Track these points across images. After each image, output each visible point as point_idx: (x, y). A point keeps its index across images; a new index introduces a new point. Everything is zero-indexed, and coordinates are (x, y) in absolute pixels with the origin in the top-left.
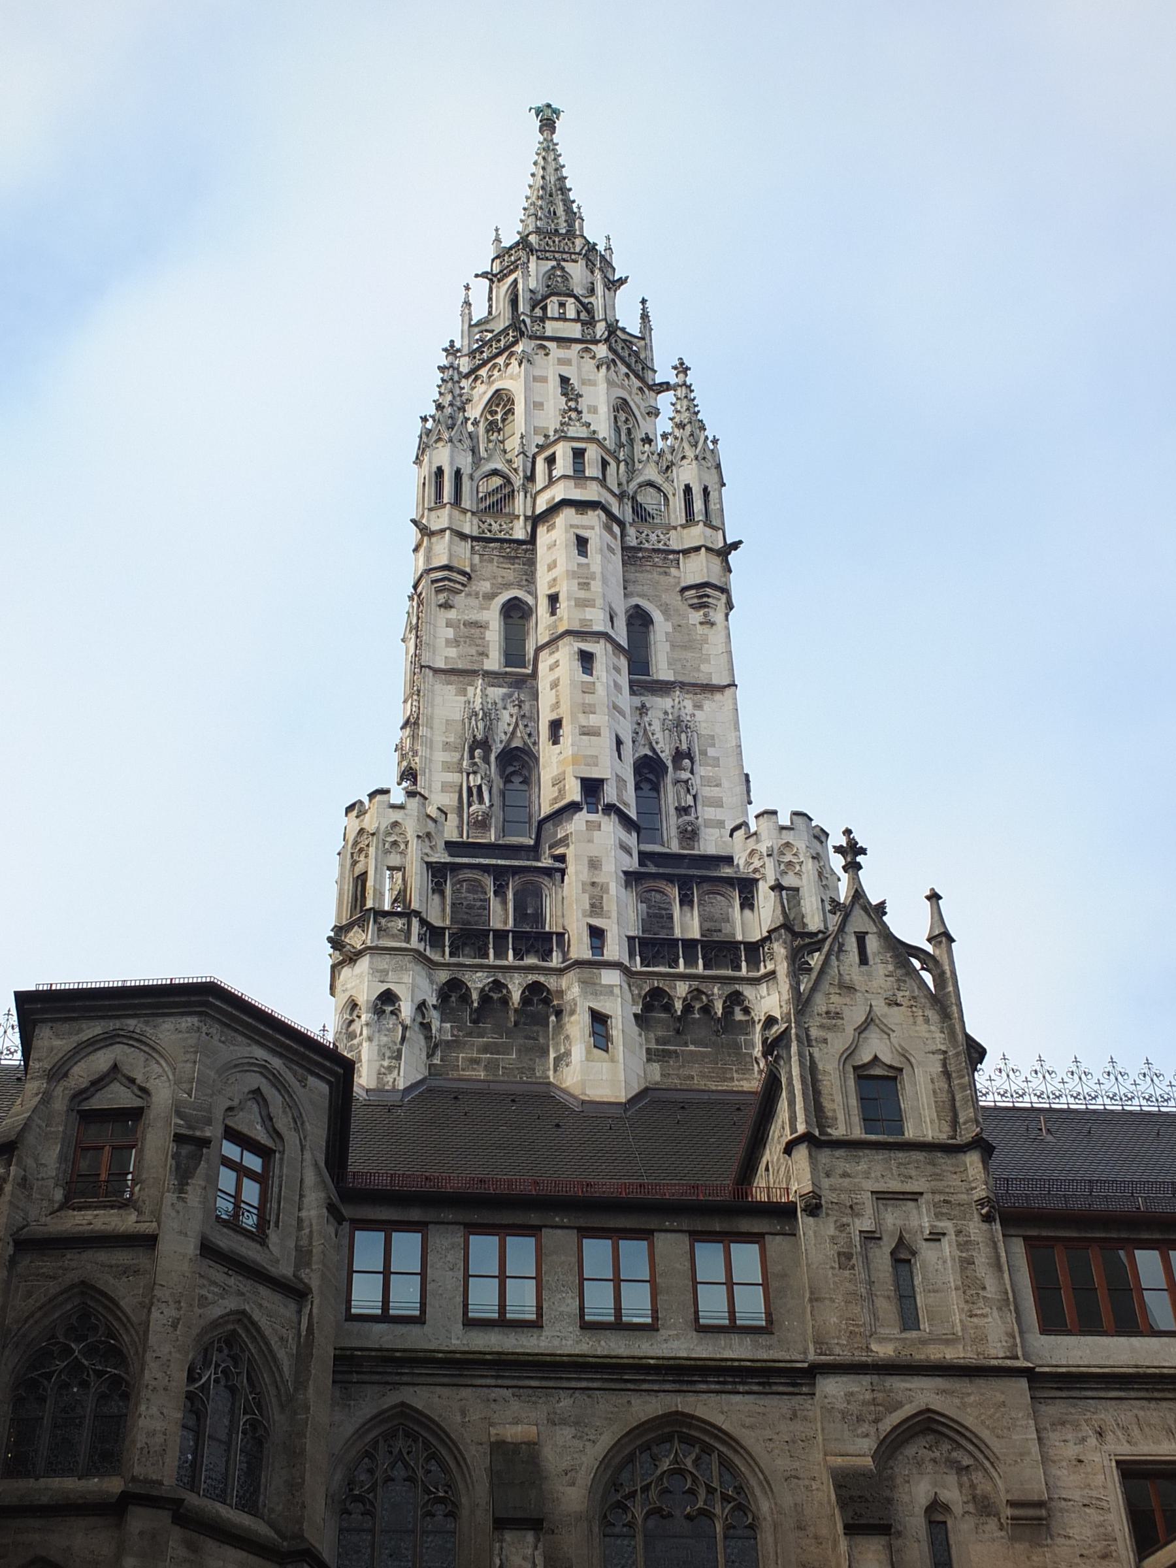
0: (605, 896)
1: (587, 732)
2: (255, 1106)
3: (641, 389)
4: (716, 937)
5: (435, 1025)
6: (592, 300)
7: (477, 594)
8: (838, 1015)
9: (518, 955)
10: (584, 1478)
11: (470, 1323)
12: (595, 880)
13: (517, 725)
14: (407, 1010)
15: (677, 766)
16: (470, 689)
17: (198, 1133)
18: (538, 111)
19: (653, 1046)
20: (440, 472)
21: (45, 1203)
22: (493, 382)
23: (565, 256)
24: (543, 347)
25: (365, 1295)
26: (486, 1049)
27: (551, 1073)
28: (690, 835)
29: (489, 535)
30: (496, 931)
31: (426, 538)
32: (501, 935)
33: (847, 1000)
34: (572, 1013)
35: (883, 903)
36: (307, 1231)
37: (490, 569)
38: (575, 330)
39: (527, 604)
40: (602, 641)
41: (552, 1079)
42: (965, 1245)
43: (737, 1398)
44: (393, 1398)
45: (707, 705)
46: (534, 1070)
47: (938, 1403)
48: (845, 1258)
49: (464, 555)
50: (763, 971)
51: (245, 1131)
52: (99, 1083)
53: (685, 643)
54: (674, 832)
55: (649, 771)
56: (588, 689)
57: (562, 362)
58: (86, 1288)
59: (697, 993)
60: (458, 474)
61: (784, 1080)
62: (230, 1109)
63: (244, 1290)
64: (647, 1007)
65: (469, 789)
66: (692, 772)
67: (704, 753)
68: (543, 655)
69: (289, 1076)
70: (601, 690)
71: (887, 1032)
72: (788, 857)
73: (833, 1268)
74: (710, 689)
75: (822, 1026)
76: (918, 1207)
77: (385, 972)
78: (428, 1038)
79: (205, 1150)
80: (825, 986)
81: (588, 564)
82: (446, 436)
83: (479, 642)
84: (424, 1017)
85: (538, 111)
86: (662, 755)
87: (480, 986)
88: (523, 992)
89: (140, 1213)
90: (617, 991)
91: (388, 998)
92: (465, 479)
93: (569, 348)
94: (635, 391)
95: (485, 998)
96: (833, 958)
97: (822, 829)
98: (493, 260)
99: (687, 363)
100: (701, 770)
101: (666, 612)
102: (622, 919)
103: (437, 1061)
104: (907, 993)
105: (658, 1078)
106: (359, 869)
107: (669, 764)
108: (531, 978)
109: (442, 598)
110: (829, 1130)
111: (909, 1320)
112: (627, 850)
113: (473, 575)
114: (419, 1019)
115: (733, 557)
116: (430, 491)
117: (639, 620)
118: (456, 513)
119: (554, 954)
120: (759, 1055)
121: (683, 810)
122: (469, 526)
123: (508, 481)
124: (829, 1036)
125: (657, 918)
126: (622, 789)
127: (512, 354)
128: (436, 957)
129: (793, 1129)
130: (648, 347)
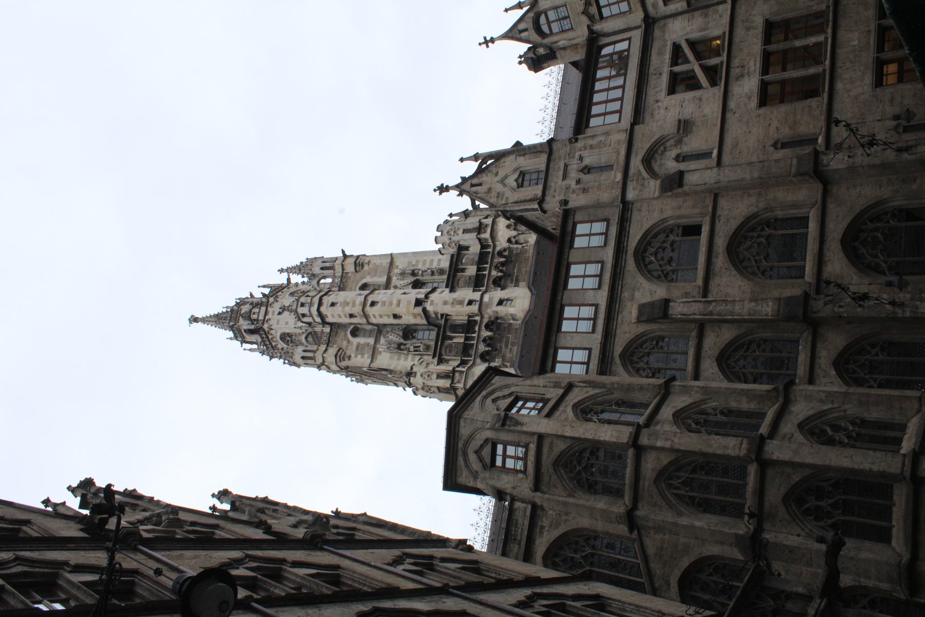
4: (477, 259)
8: (498, 194)
10: (653, 287)
11: (593, 331)
18: (191, 323)
20: (303, 358)
25: (578, 370)
26: (506, 346)
28: (441, 272)
32: (467, 339)
38: (263, 309)
42: (585, 148)
43: (631, 231)
44: (617, 360)
47: (640, 157)
48: (585, 190)
49: (332, 351)
52: (481, 460)
53: (375, 272)
55: (417, 285)
56: (384, 303)
58: (556, 464)
60: (304, 351)
64: (499, 286)
69: (490, 389)
71: (506, 177)
74: (392, 263)
80: (487, 198)
85: (191, 323)
95: (488, 345)
100: (420, 267)
101: (363, 278)
102: (466, 293)
103: (508, 364)
106: (436, 390)
108: (483, 328)
111: (609, 167)
115: (347, 253)
117: (364, 287)
121: (433, 273)
122: (323, 347)
123: (310, 333)
126: (420, 293)
128: (471, 363)
129: (536, 210)
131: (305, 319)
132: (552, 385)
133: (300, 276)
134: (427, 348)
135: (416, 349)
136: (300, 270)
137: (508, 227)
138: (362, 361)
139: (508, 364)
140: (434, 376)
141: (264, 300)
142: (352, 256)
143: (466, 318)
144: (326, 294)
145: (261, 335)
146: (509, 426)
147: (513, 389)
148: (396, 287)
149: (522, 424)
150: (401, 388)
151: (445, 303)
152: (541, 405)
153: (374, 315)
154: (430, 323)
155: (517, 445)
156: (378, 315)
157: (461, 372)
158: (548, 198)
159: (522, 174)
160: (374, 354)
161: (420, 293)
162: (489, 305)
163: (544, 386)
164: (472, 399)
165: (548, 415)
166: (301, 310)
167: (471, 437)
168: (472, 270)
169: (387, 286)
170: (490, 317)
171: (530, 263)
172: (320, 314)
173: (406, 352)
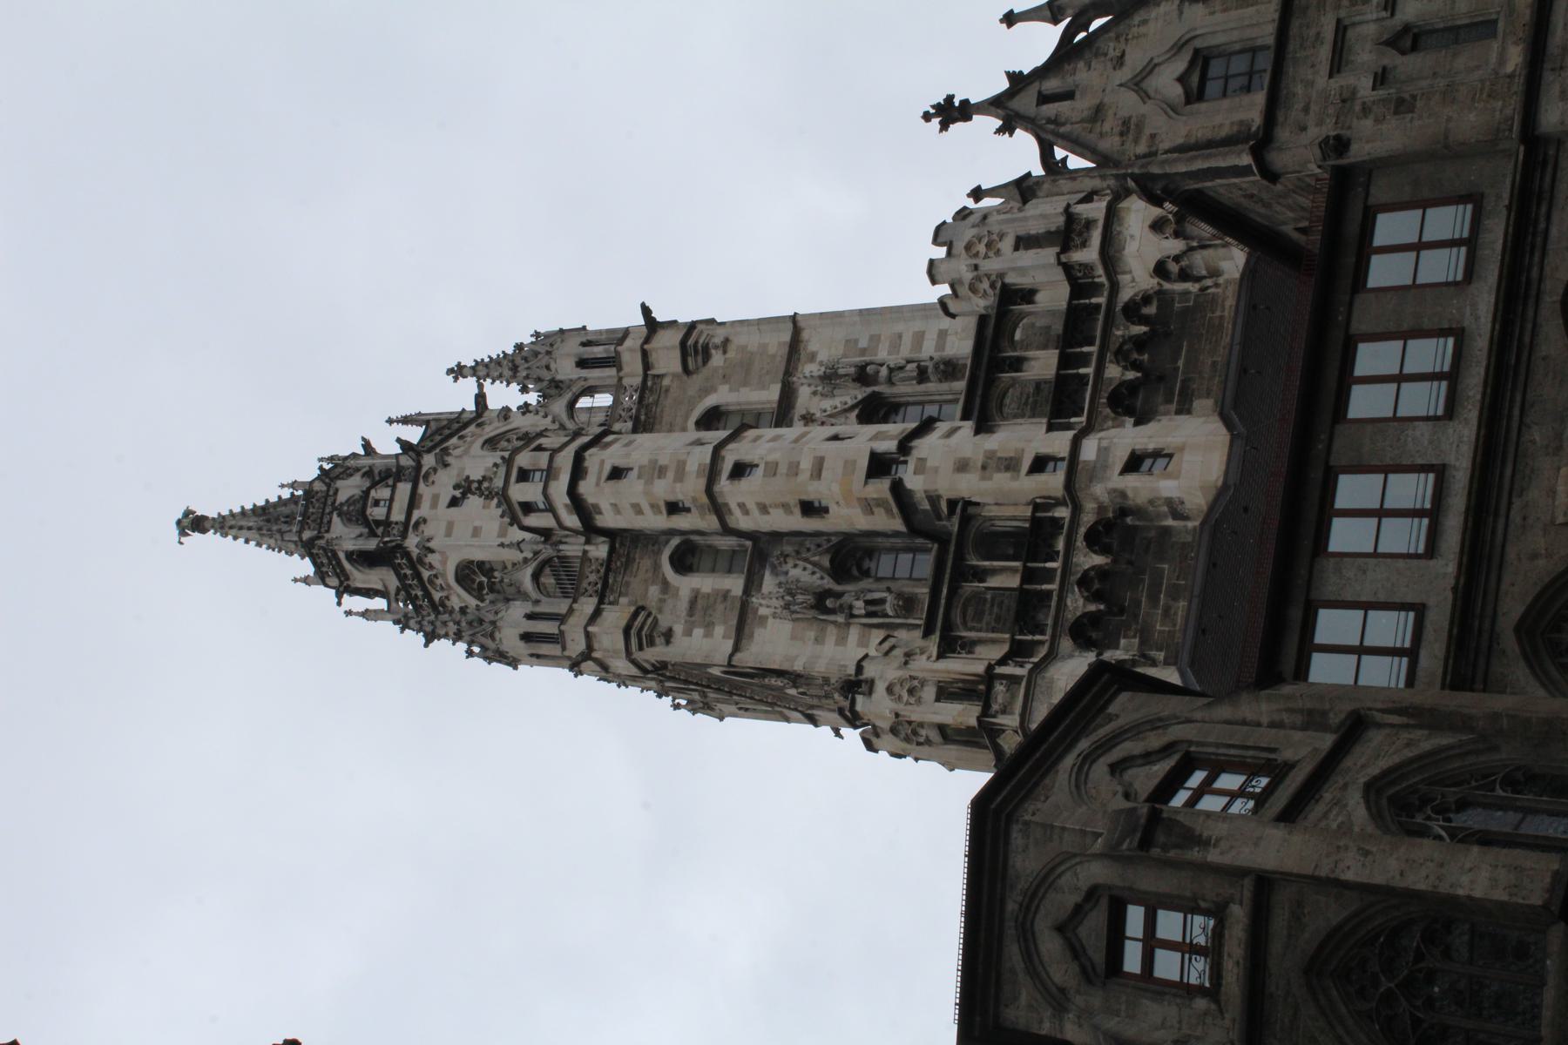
1: (818, 470)
2: (1130, 772)
4: (1058, 327)
7: (662, 601)
8: (1126, 123)
11: (1431, 550)
13: (806, 560)
16: (762, 611)
17: (1143, 821)
19: (1173, 407)
20: (527, 637)
21: (1209, 1020)
22: (449, 586)
25: (1382, 674)
26: (1154, 599)
27: (1190, 524)
28: (948, 369)
30: (1024, 580)
31: (595, 655)
32: (1029, 576)
33: (1111, 113)
34: (1123, 494)
36: (1285, 717)
37: (636, 583)
38: (404, 489)
39: (678, 547)
40: (723, 453)
41: (1197, 523)
43: (1554, 232)
44: (1509, 642)
45: (812, 347)
46: (1184, 544)
48: (1402, 106)
49: (615, 617)
50: (1103, 280)
51: (1156, 781)
52: (1076, 951)
54: (945, 386)
55: (874, 410)
56: (772, 469)
57: (434, 505)
59: (1121, 356)
60: (530, 617)
62: (1127, 796)
63: (1341, 782)
64: (1130, 412)
65: (869, 615)
67: (863, 351)
69: (1102, 732)
70: (771, 458)
71: (1151, 68)
72: (982, 248)
73: (1412, 120)
74: (795, 345)
75: (1136, 141)
76: (1354, 24)
79: (1165, 815)
80: (1091, 138)
81: (641, 467)
85: (183, 533)
87: (1081, 602)
88: (1095, 552)
89: (1231, 900)
90: (1105, 443)
92: (538, 609)
94: (478, 431)
95: (1096, 597)
96: (1062, 130)
97: (958, 213)
98: (326, 585)
99: (453, 364)
100: (882, 354)
101: (706, 391)
102: (1029, 436)
103: (1161, 656)
104: (1112, 45)
105: (1209, 403)
106: (934, 735)
107: (869, 390)
108: (1080, 542)
109: (659, 640)
111: (1483, 29)
115: (660, 316)
116: (545, 649)
117: (711, 419)
118: (572, 620)
120: (1197, 286)
121: (922, 375)
122: (587, 605)
124: (1147, 131)
126: (885, 437)
127: (420, 560)
128: (1043, 651)
132: (1298, 719)
133: (515, 387)
134: (908, 604)
135: (874, 608)
136: (515, 369)
137: (1157, 226)
138: (706, 646)
139: (1161, 656)
140: (929, 693)
141: (407, 461)
143: (1028, 512)
144: (596, 441)
145: (397, 570)
146: (1165, 848)
147: (1176, 732)
148: (808, 419)
149: (1204, 843)
150: (826, 731)
151: (962, 466)
152: (1264, 781)
153: (742, 506)
154: (914, 529)
155: (1189, 907)
156: (755, 505)
157: (1013, 680)
158: (1283, 134)
159: (1202, 60)
161: (885, 437)
162: (1097, 470)
163: (1272, 725)
164: (1048, 764)
165: (1290, 815)
166: (521, 492)
167: (1045, 881)
168: (1043, 364)
169: (783, 414)
170: (1101, 508)
171: (1226, 340)
172: (578, 504)
173: (840, 619)
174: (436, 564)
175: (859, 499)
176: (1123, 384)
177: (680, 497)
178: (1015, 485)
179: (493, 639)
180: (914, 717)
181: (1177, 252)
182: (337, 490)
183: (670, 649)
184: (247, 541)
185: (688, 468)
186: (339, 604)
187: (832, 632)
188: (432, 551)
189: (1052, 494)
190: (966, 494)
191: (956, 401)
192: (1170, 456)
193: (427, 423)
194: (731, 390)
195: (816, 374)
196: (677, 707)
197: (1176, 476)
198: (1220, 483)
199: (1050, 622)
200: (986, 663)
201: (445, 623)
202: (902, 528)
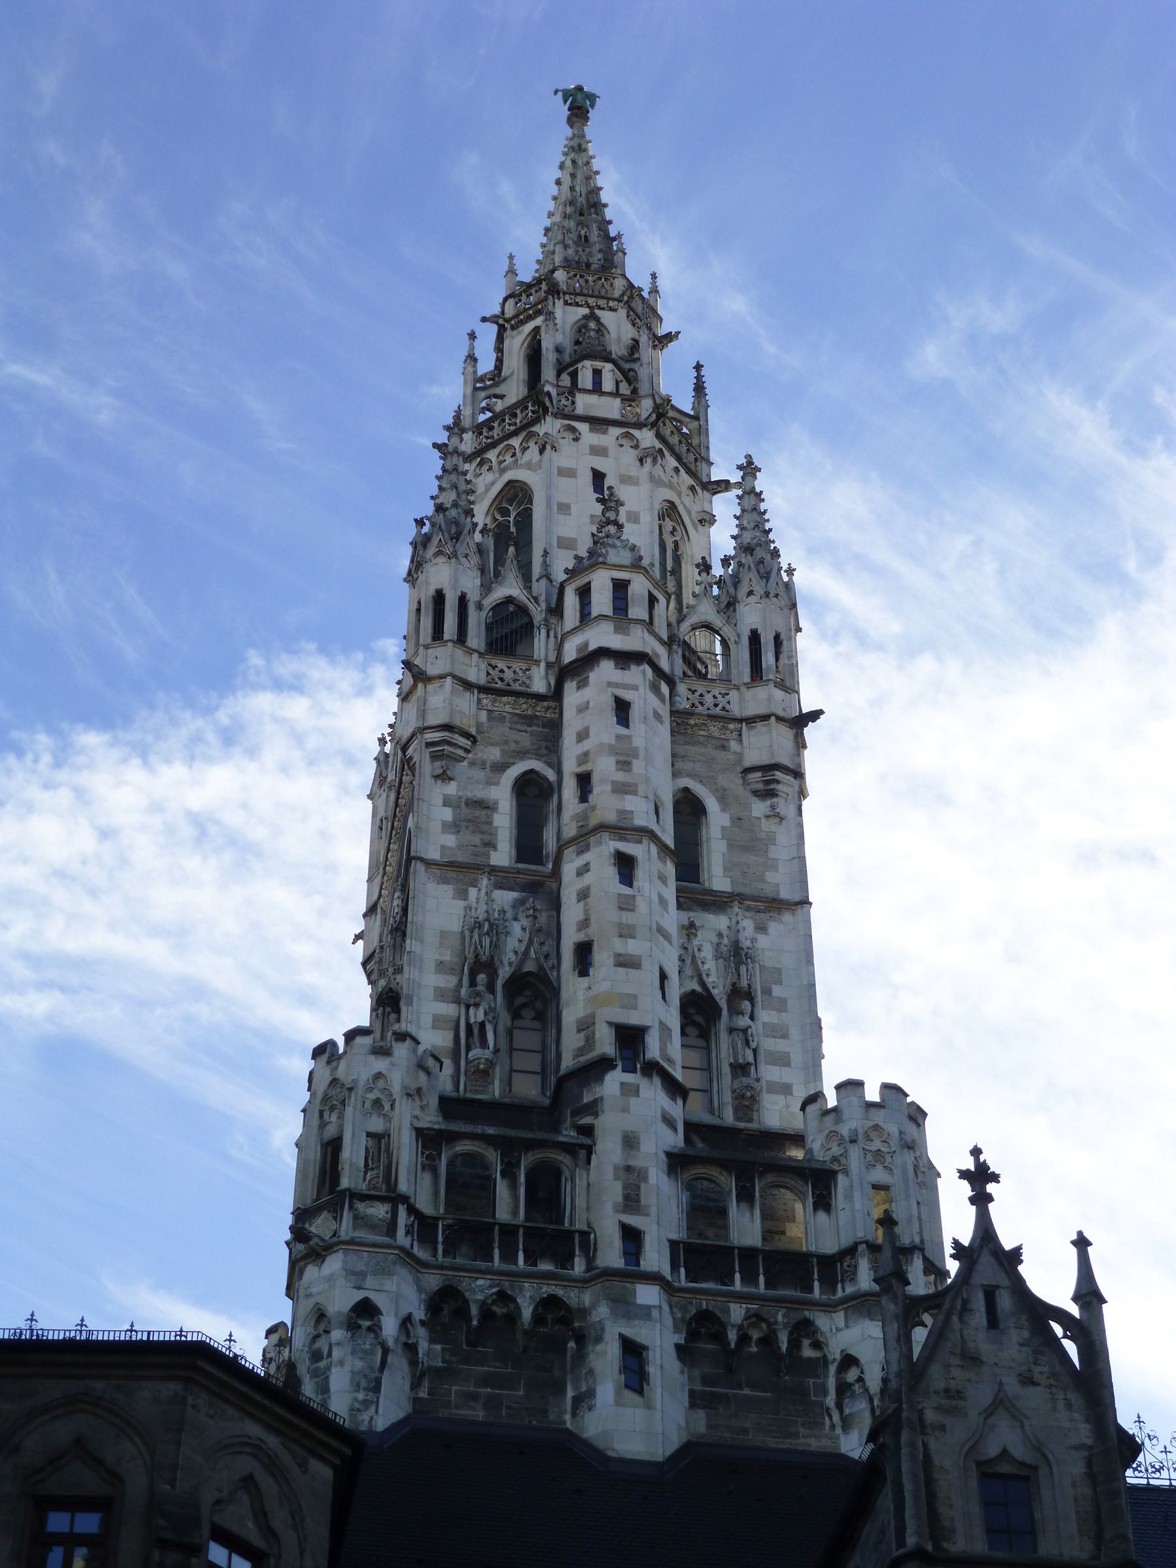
0: (643, 1186)
1: (626, 962)
3: (692, 488)
5: (423, 1346)
6: (635, 366)
8: (959, 1395)
9: (531, 1259)
12: (631, 1163)
14: (389, 1327)
15: (735, 1011)
18: (567, 95)
19: (698, 1387)
20: (439, 598)
22: (503, 471)
23: (601, 302)
24: (573, 430)
27: (568, 1417)
28: (747, 1103)
29: (500, 685)
31: (420, 685)
32: (509, 1231)
34: (599, 1339)
35: (1019, 1248)
38: (611, 408)
39: (545, 779)
40: (645, 841)
41: (569, 1425)
45: (773, 927)
49: (467, 709)
53: (748, 842)
54: (728, 1097)
55: (699, 1012)
56: (626, 905)
59: (755, 1318)
60: (463, 601)
61: (889, 1476)
62: (218, 1502)
64: (692, 1335)
65: (469, 1027)
66: (752, 1018)
67: (767, 992)
68: (569, 853)
70: (641, 905)
71: (1017, 1416)
72: (877, 1145)
75: (939, 1409)
77: (362, 1275)
78: (414, 1362)
81: (629, 737)
82: (448, 549)
83: (485, 828)
84: (408, 1336)
85: (567, 95)
86: (715, 992)
87: (480, 1297)
90: (655, 1313)
91: (366, 1310)
93: (605, 432)
94: (684, 490)
95: (487, 1314)
96: (955, 1318)
97: (919, 1109)
98: (505, 300)
100: (766, 1016)
101: (723, 799)
102: (664, 1218)
103: (423, 1394)
104: (1046, 1369)
105: (702, 1428)
106: (330, 1132)
107: (723, 1004)
108: (547, 1289)
110: (945, 1545)
112: (669, 1121)
113: (479, 738)
114: (403, 1339)
115: (810, 731)
116: (427, 622)
117: (689, 810)
118: (459, 653)
119: (577, 1260)
121: (740, 1069)
122: (475, 671)
125: (705, 1210)
127: (532, 435)
129: (901, 1543)
130: (703, 431)
131: (571, 600)
134: (483, 1074)
139: (423, 1394)
140: (376, 1124)
142: (800, 744)
143: (580, 1225)
145: (522, 404)
148: (690, 929)
150: (359, 926)
151: (630, 1142)
153: (583, 870)
160: (460, 871)
161: (667, 1044)
162: (625, 1307)
166: (601, 583)
170: (584, 1312)
171: (773, 1443)
172: (590, 658)
174: (527, 456)
175: (593, 1016)
176: (723, 1326)
177: (596, 790)
178: (609, 1208)
179: (436, 555)
180: (349, 1111)
181: (868, 1383)
182: (615, 310)
183: (428, 781)
184: (558, 182)
185: (627, 797)
186: (484, 319)
187: (452, 981)
188: (542, 450)
189: (599, 1254)
190: (600, 1147)
191: (712, 1112)
192: (640, 1392)
193: (696, 418)
194: (724, 828)
195: (741, 937)
196: (382, 741)
197: (619, 1402)
198: (610, 1453)
199: (459, 1261)
200: (411, 1193)
201: (455, 487)
202: (563, 1071)
